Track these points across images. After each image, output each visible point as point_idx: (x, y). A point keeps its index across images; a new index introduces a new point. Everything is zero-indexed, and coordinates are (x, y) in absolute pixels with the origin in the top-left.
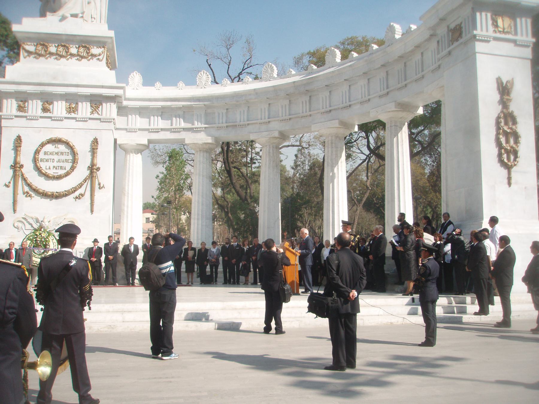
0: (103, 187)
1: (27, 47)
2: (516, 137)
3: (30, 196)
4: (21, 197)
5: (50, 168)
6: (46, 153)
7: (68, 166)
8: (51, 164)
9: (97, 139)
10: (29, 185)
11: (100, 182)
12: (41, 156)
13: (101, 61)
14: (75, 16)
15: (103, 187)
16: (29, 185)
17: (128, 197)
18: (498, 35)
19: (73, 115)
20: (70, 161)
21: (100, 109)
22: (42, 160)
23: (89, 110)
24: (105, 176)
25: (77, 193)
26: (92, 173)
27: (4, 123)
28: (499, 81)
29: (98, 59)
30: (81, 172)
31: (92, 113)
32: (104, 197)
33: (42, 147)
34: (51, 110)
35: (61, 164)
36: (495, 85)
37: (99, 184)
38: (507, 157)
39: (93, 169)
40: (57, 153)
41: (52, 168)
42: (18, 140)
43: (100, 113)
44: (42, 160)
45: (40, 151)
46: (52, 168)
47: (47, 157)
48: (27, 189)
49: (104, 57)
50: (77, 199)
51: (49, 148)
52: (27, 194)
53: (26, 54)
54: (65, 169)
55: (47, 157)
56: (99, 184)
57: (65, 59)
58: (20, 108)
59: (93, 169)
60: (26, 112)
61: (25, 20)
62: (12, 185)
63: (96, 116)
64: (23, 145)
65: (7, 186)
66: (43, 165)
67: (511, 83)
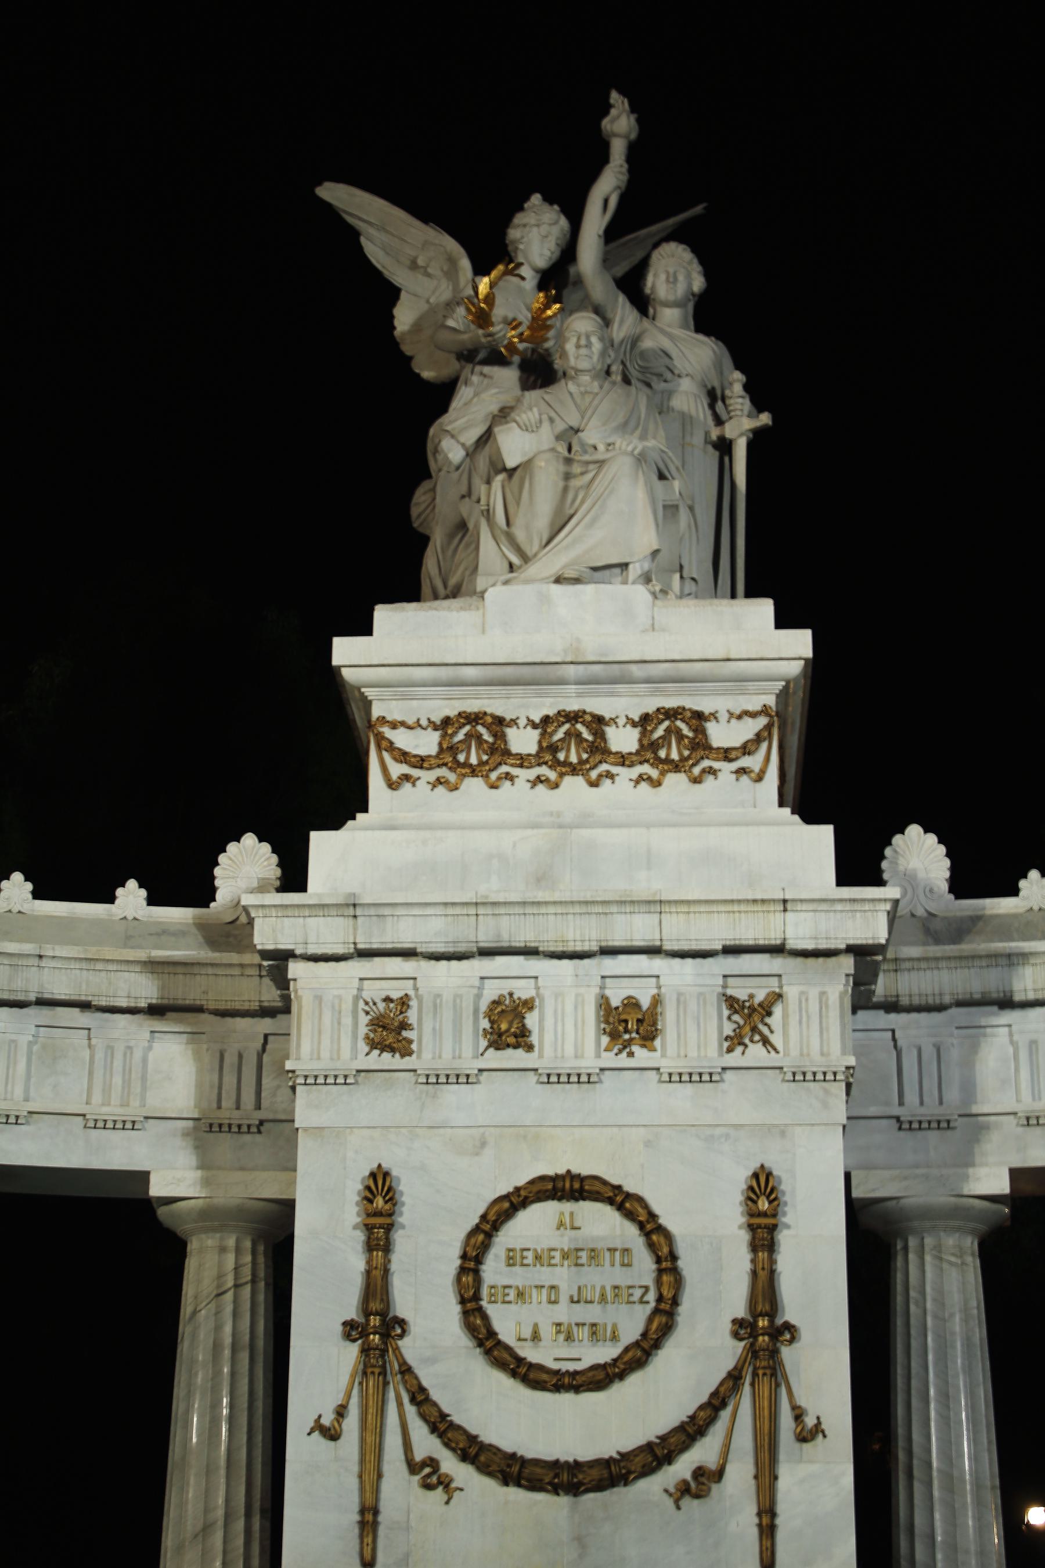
0: (818, 1430)
1: (401, 739)
4: (398, 1488)
5: (536, 1337)
6: (512, 1259)
8: (543, 1315)
9: (769, 1175)
11: (802, 1401)
13: (759, 778)
15: (818, 1430)
16: (441, 1425)
17: (929, 1484)
19: (642, 1055)
20: (638, 1293)
21: (776, 1019)
25: (682, 1467)
26: (753, 1352)
27: (308, 1110)
29: (742, 771)
31: (735, 1041)
32: (821, 1486)
33: (496, 1226)
34: (534, 1039)
35: (592, 1313)
37: (799, 1415)
41: (547, 1331)
42: (380, 1192)
43: (776, 1039)
45: (485, 1247)
46: (547, 1331)
47: (518, 1277)
48: (426, 1444)
49: (767, 760)
50: (687, 1502)
52: (429, 1475)
53: (397, 769)
54: (615, 1338)
55: (518, 1277)
56: (799, 1415)
57: (579, 781)
60: (407, 1053)
61: (382, 614)
62: (351, 1424)
65: (332, 1434)
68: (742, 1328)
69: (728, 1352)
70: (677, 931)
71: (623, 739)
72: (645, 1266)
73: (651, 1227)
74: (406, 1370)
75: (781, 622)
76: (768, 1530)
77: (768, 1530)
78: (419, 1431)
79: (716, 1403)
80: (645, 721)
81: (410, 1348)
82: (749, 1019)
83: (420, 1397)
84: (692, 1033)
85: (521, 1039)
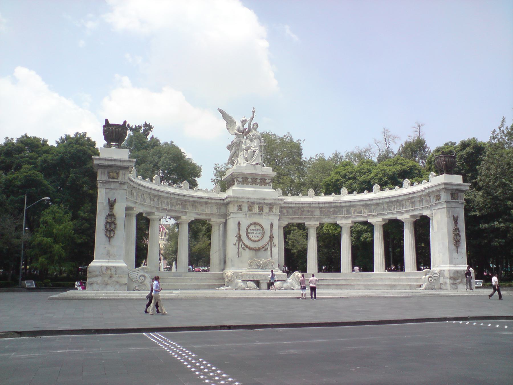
1: (238, 179)
2: (460, 236)
3: (245, 250)
6: (250, 230)
7: (260, 236)
8: (253, 235)
10: (244, 244)
12: (249, 231)
14: (257, 164)
18: (453, 200)
22: (249, 233)
23: (268, 210)
24: (276, 241)
28: (454, 216)
30: (267, 238)
31: (269, 211)
35: (257, 235)
36: (452, 218)
38: (457, 243)
39: (271, 237)
40: (255, 230)
42: (239, 223)
44: (249, 233)
47: (251, 231)
48: (243, 246)
51: (252, 227)
52: (243, 249)
55: (251, 231)
58: (240, 208)
59: (271, 237)
63: (271, 213)
64: (241, 225)
65: (235, 245)
66: (250, 235)
67: (457, 217)
68: (270, 237)
69: (269, 239)
70: (266, 201)
71: (258, 181)
72: (262, 231)
73: (262, 227)
74: (242, 240)
75: (273, 170)
76: (271, 253)
77: (271, 253)
78: (242, 245)
79: (268, 243)
80: (260, 179)
81: (242, 238)
82: (271, 209)
83: (242, 242)
84: (266, 210)
85: (252, 211)
